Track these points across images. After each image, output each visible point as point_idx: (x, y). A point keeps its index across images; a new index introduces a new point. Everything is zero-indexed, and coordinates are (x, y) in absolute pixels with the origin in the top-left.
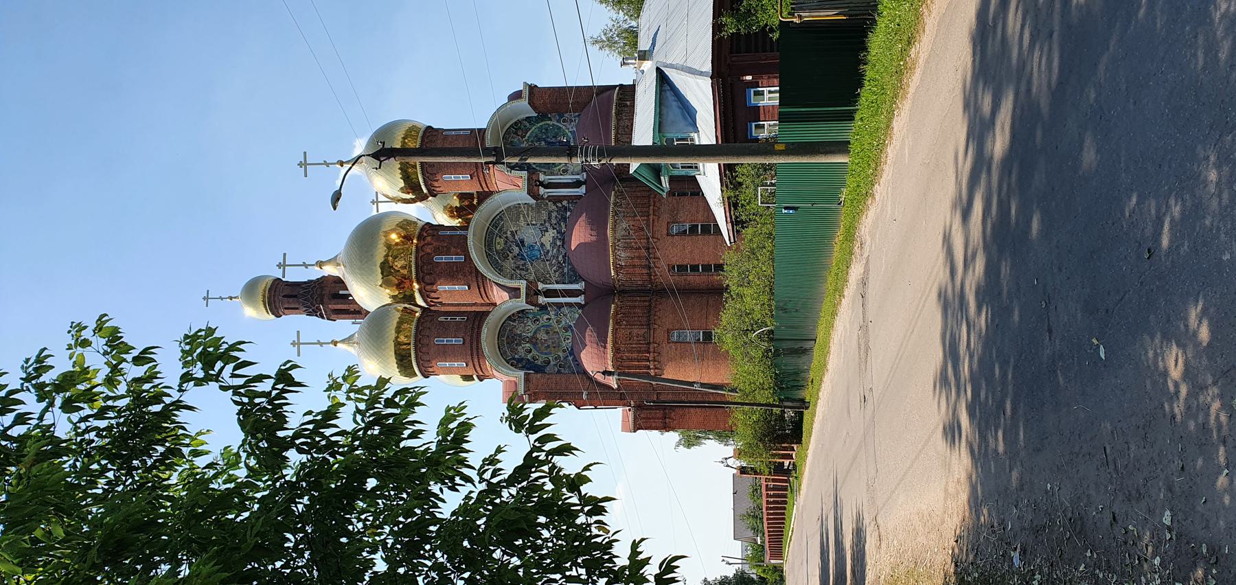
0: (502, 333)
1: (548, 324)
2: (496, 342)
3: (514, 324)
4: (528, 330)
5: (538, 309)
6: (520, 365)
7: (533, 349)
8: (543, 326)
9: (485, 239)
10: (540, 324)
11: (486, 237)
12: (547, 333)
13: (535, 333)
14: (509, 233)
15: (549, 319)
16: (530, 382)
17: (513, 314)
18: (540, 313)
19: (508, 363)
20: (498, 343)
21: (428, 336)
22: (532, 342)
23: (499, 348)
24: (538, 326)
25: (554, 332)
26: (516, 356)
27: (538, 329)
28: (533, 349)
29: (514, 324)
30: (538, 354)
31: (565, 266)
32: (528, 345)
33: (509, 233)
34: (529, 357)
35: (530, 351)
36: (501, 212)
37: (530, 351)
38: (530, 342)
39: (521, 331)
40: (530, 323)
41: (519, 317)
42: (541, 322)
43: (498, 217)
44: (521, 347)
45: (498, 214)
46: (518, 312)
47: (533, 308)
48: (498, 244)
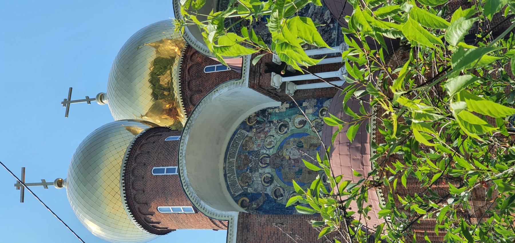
0: (231, 150)
2: (221, 165)
3: (250, 134)
4: (270, 143)
5: (288, 105)
6: (255, 206)
7: (276, 177)
8: (292, 136)
10: (289, 132)
12: (300, 146)
13: (281, 147)
15: (304, 122)
16: (248, 231)
17: (249, 118)
18: (291, 112)
19: (237, 201)
20: (224, 168)
21: (145, 165)
22: (274, 164)
23: (225, 175)
24: (286, 136)
25: (311, 145)
26: (250, 190)
27: (285, 142)
28: (276, 177)
29: (250, 134)
30: (282, 184)
31: (334, 28)
32: (268, 170)
34: (269, 190)
35: (270, 181)
37: (270, 181)
38: (272, 165)
39: (259, 145)
40: (273, 132)
41: (258, 122)
42: (291, 127)
44: (257, 174)
46: (257, 114)
47: (278, 104)
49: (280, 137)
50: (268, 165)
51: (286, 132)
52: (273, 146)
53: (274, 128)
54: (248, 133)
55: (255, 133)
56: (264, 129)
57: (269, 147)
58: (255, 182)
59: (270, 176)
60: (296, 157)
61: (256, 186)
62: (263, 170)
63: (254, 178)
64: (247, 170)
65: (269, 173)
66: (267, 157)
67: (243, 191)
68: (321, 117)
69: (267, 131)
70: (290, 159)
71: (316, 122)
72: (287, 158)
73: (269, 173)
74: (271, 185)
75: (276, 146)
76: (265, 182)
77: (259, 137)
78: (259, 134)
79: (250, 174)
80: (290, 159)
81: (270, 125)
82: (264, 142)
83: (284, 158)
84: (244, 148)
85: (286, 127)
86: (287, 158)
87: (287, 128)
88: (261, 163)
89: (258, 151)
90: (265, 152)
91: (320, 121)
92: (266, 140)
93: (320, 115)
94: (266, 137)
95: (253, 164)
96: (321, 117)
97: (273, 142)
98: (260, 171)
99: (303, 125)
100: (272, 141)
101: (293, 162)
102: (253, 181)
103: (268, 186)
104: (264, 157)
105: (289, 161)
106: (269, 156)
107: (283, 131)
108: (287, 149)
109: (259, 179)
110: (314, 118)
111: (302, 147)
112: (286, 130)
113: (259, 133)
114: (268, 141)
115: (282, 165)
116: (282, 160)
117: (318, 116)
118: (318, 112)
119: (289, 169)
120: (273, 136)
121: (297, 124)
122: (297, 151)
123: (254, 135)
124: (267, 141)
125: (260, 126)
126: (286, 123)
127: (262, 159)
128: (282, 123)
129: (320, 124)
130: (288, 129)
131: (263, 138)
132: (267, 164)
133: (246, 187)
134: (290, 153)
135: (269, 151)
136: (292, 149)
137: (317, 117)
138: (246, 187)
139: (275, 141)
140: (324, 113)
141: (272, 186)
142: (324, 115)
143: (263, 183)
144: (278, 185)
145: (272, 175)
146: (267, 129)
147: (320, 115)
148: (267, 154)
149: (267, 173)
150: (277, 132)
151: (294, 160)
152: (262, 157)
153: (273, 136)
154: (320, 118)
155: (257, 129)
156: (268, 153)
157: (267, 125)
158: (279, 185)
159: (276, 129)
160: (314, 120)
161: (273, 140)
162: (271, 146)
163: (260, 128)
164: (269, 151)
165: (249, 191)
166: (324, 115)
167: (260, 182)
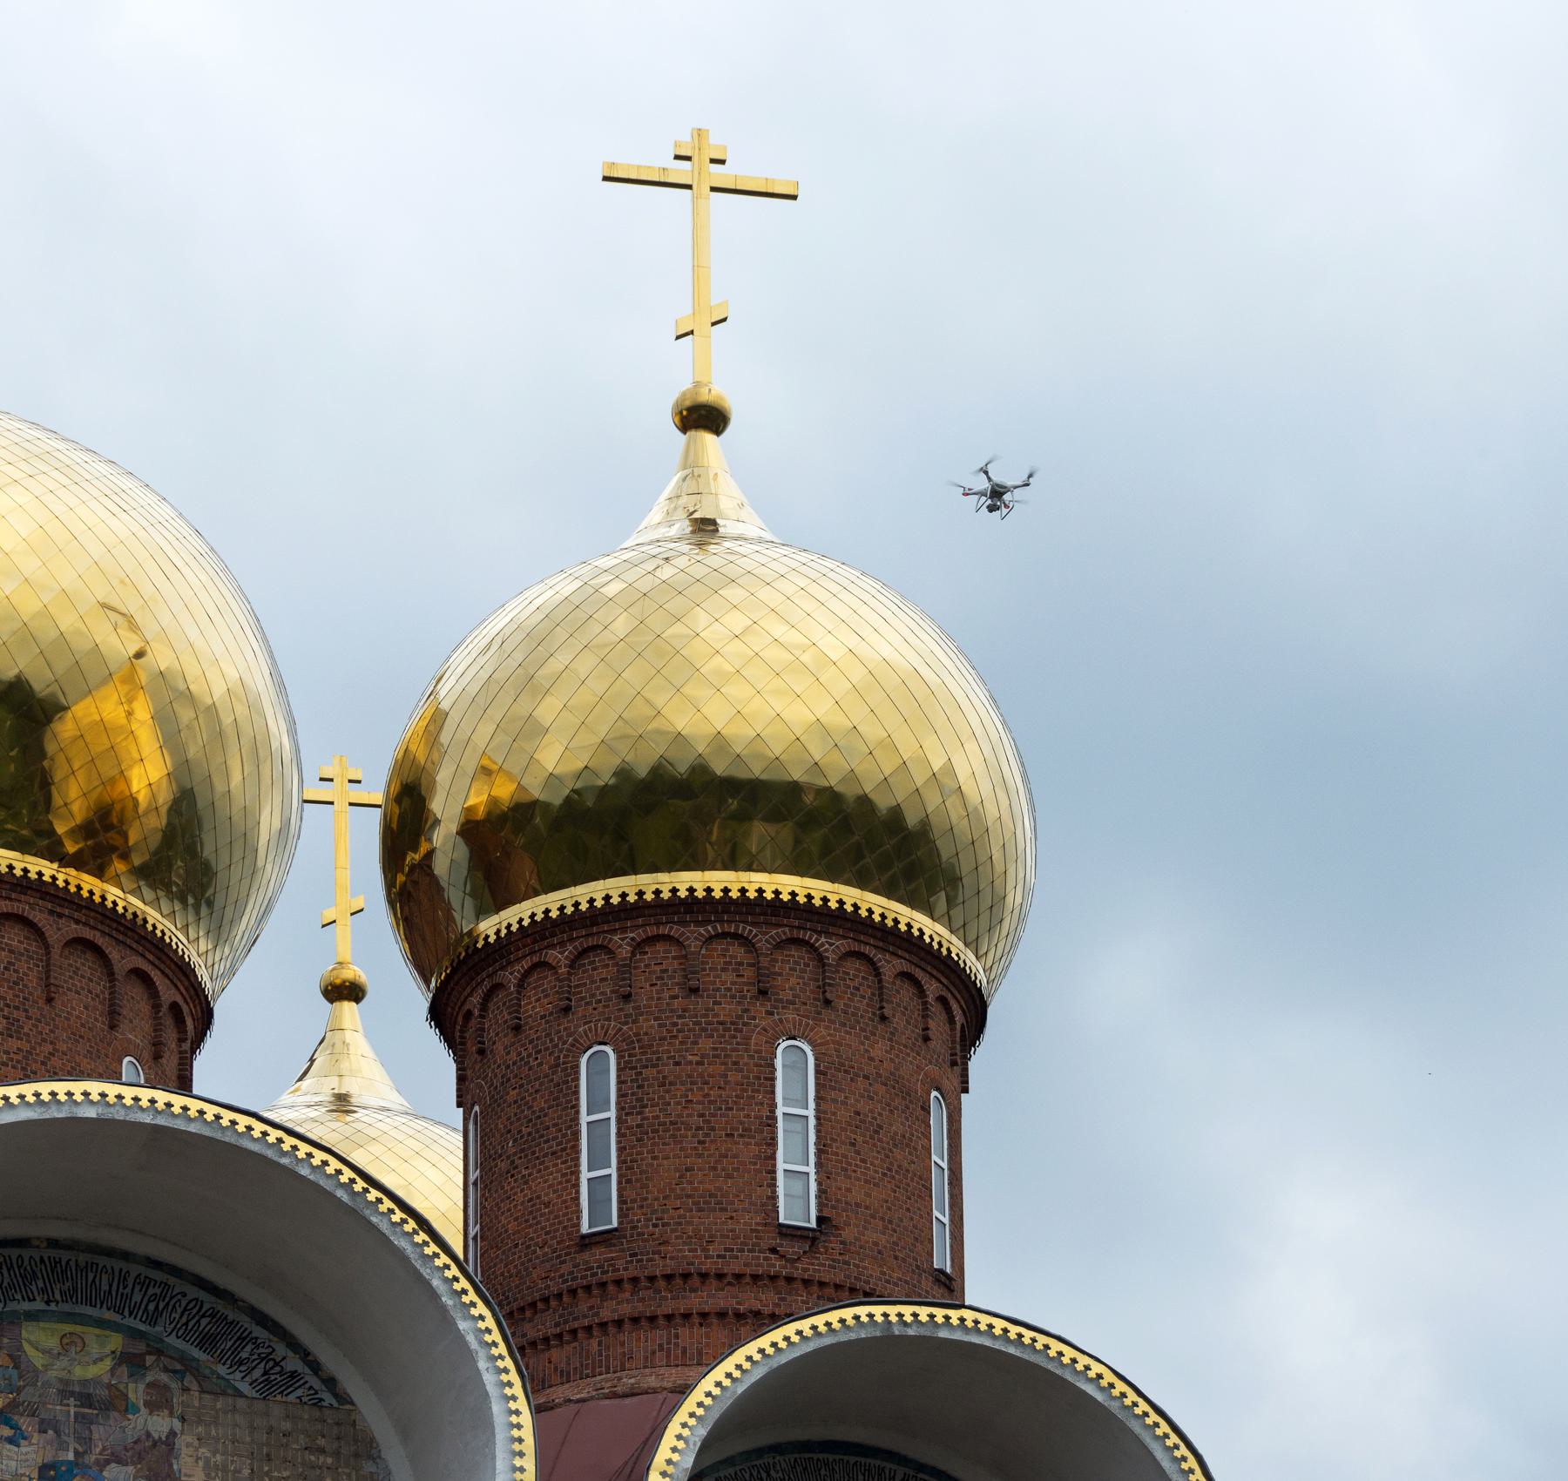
9: (110, 1252)
11: (126, 1256)
14: (160, 1425)
33: (160, 1425)
36: (331, 1383)
43: (293, 1363)
45: (315, 1367)
48: (67, 1342)
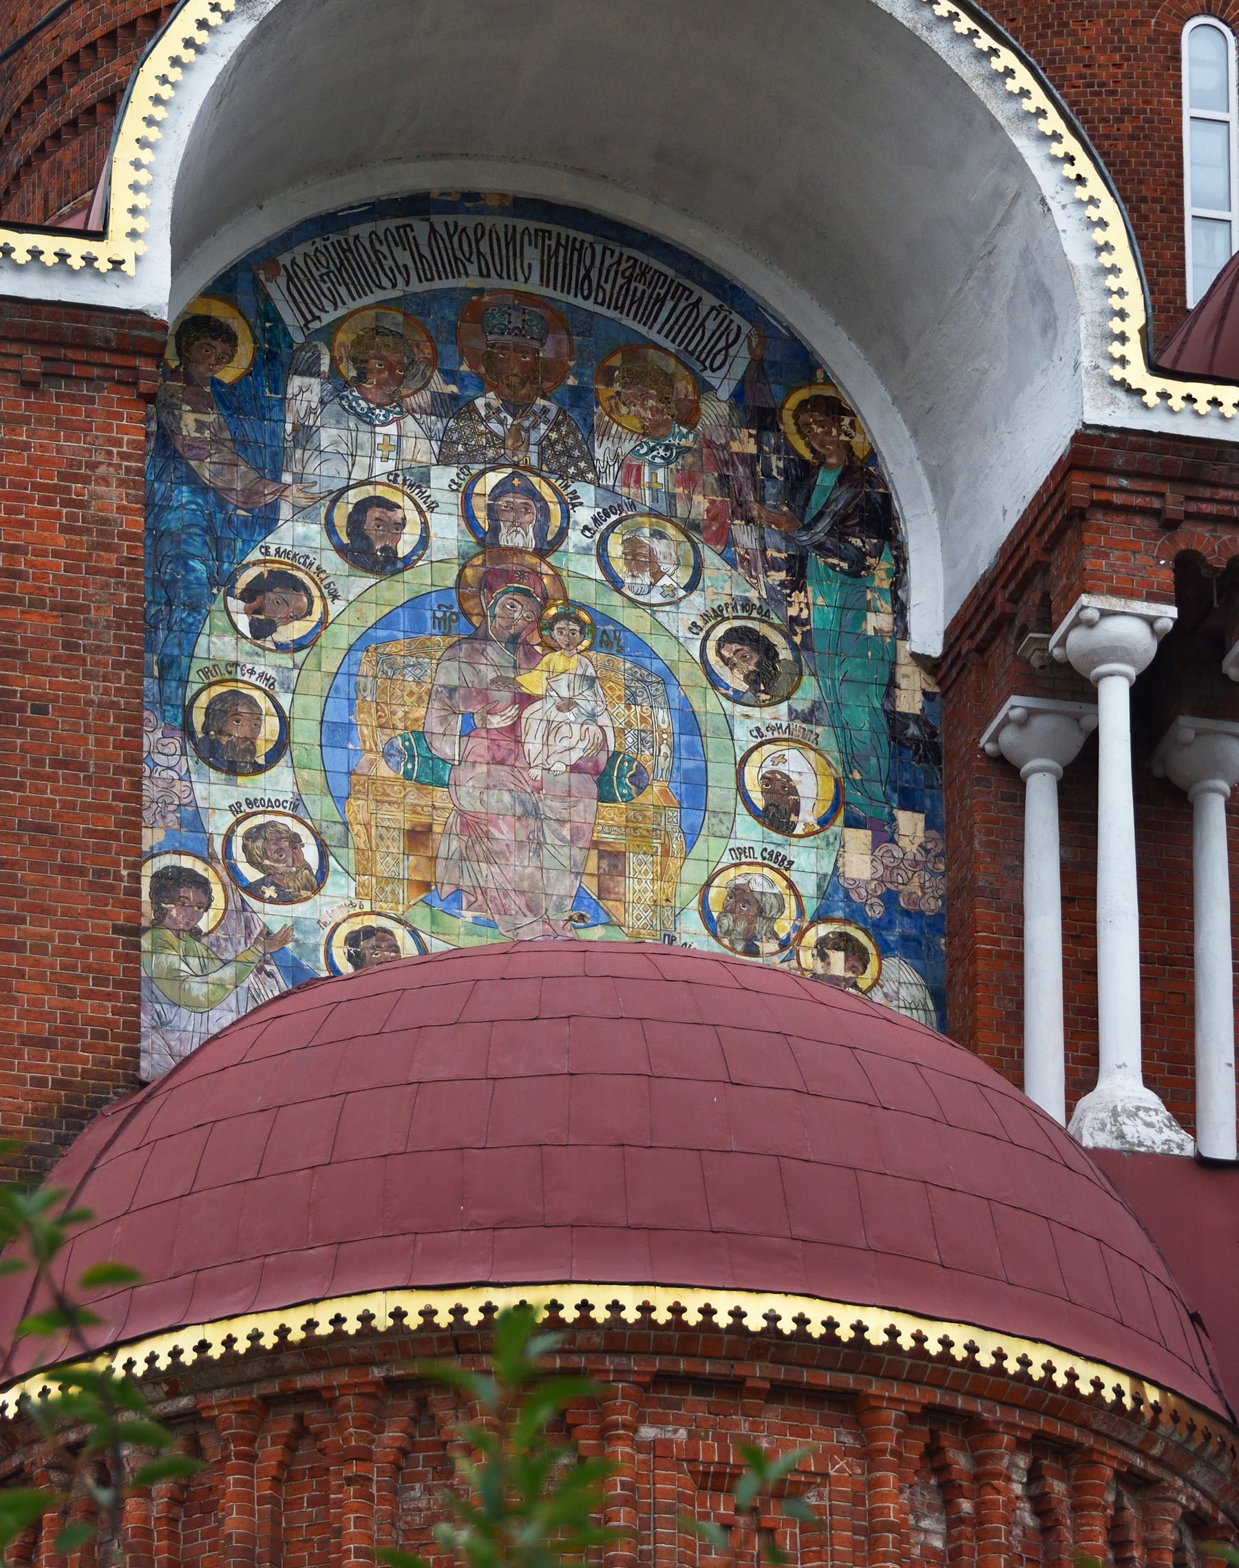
1: (720, 791)
8: (689, 723)
24: (689, 673)
29: (715, 411)
44: (420, 450)
49: (683, 632)
50: (487, 541)
51: (715, 681)
52: (615, 583)
53: (753, 595)
54: (724, 393)
55: (725, 447)
56: (749, 521)
57: (615, 548)
58: (364, 437)
59: (403, 549)
60: (533, 746)
61: (327, 436)
62: (449, 501)
63: (392, 429)
64: (450, 376)
65: (424, 541)
66: (541, 532)
67: (299, 338)
68: (811, 937)
69: (730, 542)
70: (524, 700)
71: (779, 897)
72: (532, 682)
73: (424, 541)
74: (340, 549)
75: (616, 599)
76: (362, 507)
77: (689, 480)
78: (711, 478)
79: (423, 399)
80: (524, 700)
81: (773, 565)
82: (652, 513)
83: (532, 658)
84: (616, 361)
85: (754, 680)
86: (532, 682)
87: (744, 687)
88: (500, 490)
89: (589, 470)
90: (583, 515)
91: (784, 927)
92: (671, 531)
93: (823, 930)
94: (689, 527)
95: (495, 426)
96: (811, 937)
97: (646, 579)
98: (442, 477)
99: (759, 801)
100: (657, 575)
101: (496, 722)
102: (366, 419)
103: (330, 528)
104: (545, 512)
105: (505, 695)
106: (547, 547)
107: (726, 661)
108: (591, 681)
109: (380, 468)
110: (808, 887)
111: (605, 796)
112: (736, 680)
113: (723, 480)
114: (660, 547)
115: (479, 637)
116: (514, 642)
117: (821, 917)
118: (846, 921)
119: (452, 690)
120: (691, 587)
121: (768, 766)
122: (575, 756)
123: (709, 444)
124: (659, 535)
125: (771, 490)
126: (782, 684)
127: (534, 494)
128: (785, 654)
129: (760, 926)
130: (737, 698)
131: (681, 510)
132: (495, 530)
133: (325, 366)
134: (567, 705)
135: (585, 551)
136: (593, 717)
137: (810, 906)
138: (325, 366)
139: (656, 597)
140: (838, 960)
141: (332, 562)
142: (823, 957)
143: (354, 496)
144: (335, 608)
145: (408, 562)
146: (745, 537)
147: (823, 930)
148: (562, 534)
149: (425, 527)
150: (718, 615)
151: (513, 730)
152: (546, 491)
153: (691, 587)
154: (801, 933)
155: (749, 461)
156: (575, 537)
157: (773, 539)
158: (335, 608)
159: (747, 605)
160: (791, 885)
161: (665, 581)
162: (619, 566)
163: (759, 488)
164: (585, 551)
165: (296, 382)
166: (823, 957)
167: (359, 474)
